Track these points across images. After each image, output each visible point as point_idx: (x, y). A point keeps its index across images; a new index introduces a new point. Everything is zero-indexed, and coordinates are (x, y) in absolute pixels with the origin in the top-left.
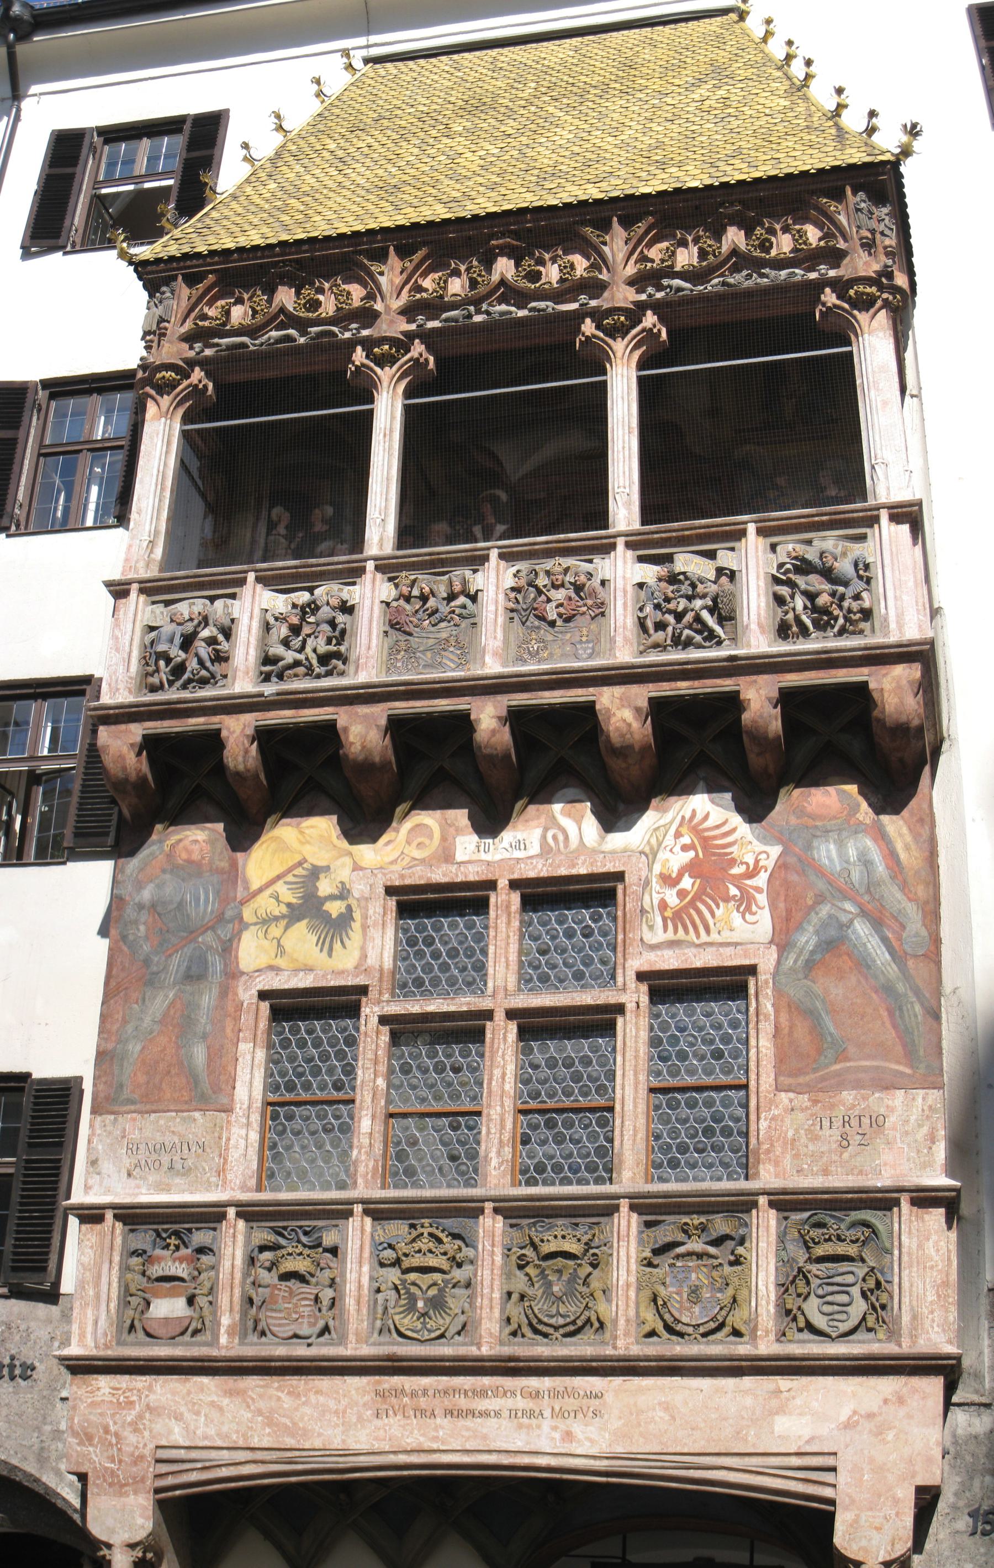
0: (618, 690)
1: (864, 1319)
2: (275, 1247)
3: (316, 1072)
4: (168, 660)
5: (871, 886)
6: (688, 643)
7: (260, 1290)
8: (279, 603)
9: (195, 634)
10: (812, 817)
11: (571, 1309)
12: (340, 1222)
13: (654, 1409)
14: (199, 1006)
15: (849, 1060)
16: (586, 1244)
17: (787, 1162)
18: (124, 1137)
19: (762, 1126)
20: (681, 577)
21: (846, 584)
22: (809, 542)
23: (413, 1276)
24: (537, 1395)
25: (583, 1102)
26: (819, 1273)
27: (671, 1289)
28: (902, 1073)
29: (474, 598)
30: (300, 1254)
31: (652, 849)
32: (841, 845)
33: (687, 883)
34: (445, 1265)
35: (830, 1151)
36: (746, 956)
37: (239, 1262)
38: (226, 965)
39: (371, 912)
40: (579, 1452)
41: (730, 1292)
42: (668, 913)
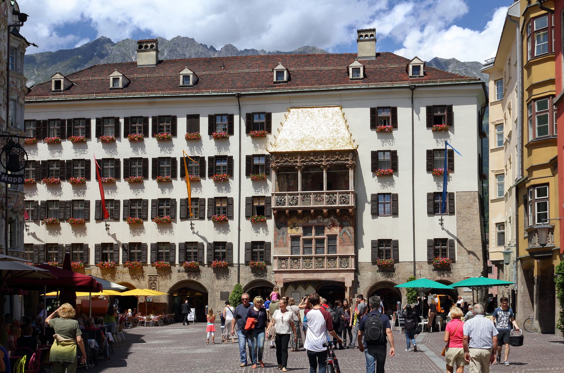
6: (331, 204)
8: (291, 197)
11: (321, 265)
19: (338, 249)
33: (331, 226)
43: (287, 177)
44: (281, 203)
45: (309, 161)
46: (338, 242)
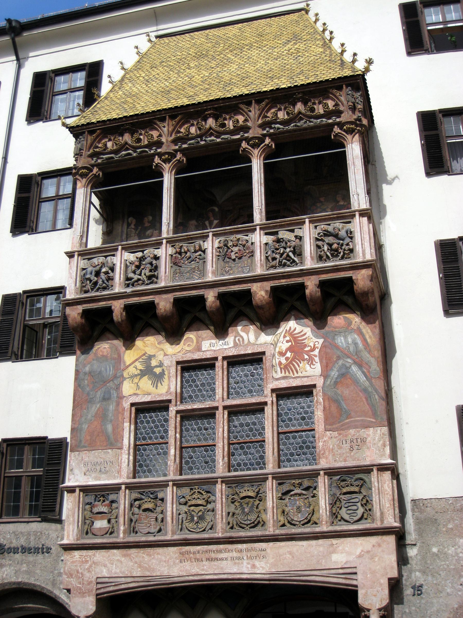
0: (259, 284)
1: (363, 516)
2: (141, 499)
3: (154, 432)
4: (91, 281)
5: (357, 352)
6: (285, 265)
7: (135, 516)
8: (131, 257)
9: (100, 270)
10: (335, 328)
11: (253, 517)
12: (164, 489)
13: (286, 554)
14: (108, 410)
15: (352, 418)
16: (257, 493)
17: (330, 457)
18: (82, 460)
19: (320, 444)
20: (281, 240)
21: (343, 240)
22: (329, 225)
23: (192, 508)
24: (241, 551)
25: (254, 439)
26: (345, 498)
27: (290, 508)
28: (372, 421)
29: (204, 252)
30: (150, 502)
31: (275, 342)
32: (345, 337)
33: (289, 354)
34: (205, 504)
35: (346, 453)
36: (312, 381)
37: (127, 506)
38: (118, 394)
39: (171, 371)
40: (258, 572)
41: (312, 508)
42: (282, 366)
43: (140, 222)
44: (96, 283)
45: (201, 136)
46: (319, 414)
